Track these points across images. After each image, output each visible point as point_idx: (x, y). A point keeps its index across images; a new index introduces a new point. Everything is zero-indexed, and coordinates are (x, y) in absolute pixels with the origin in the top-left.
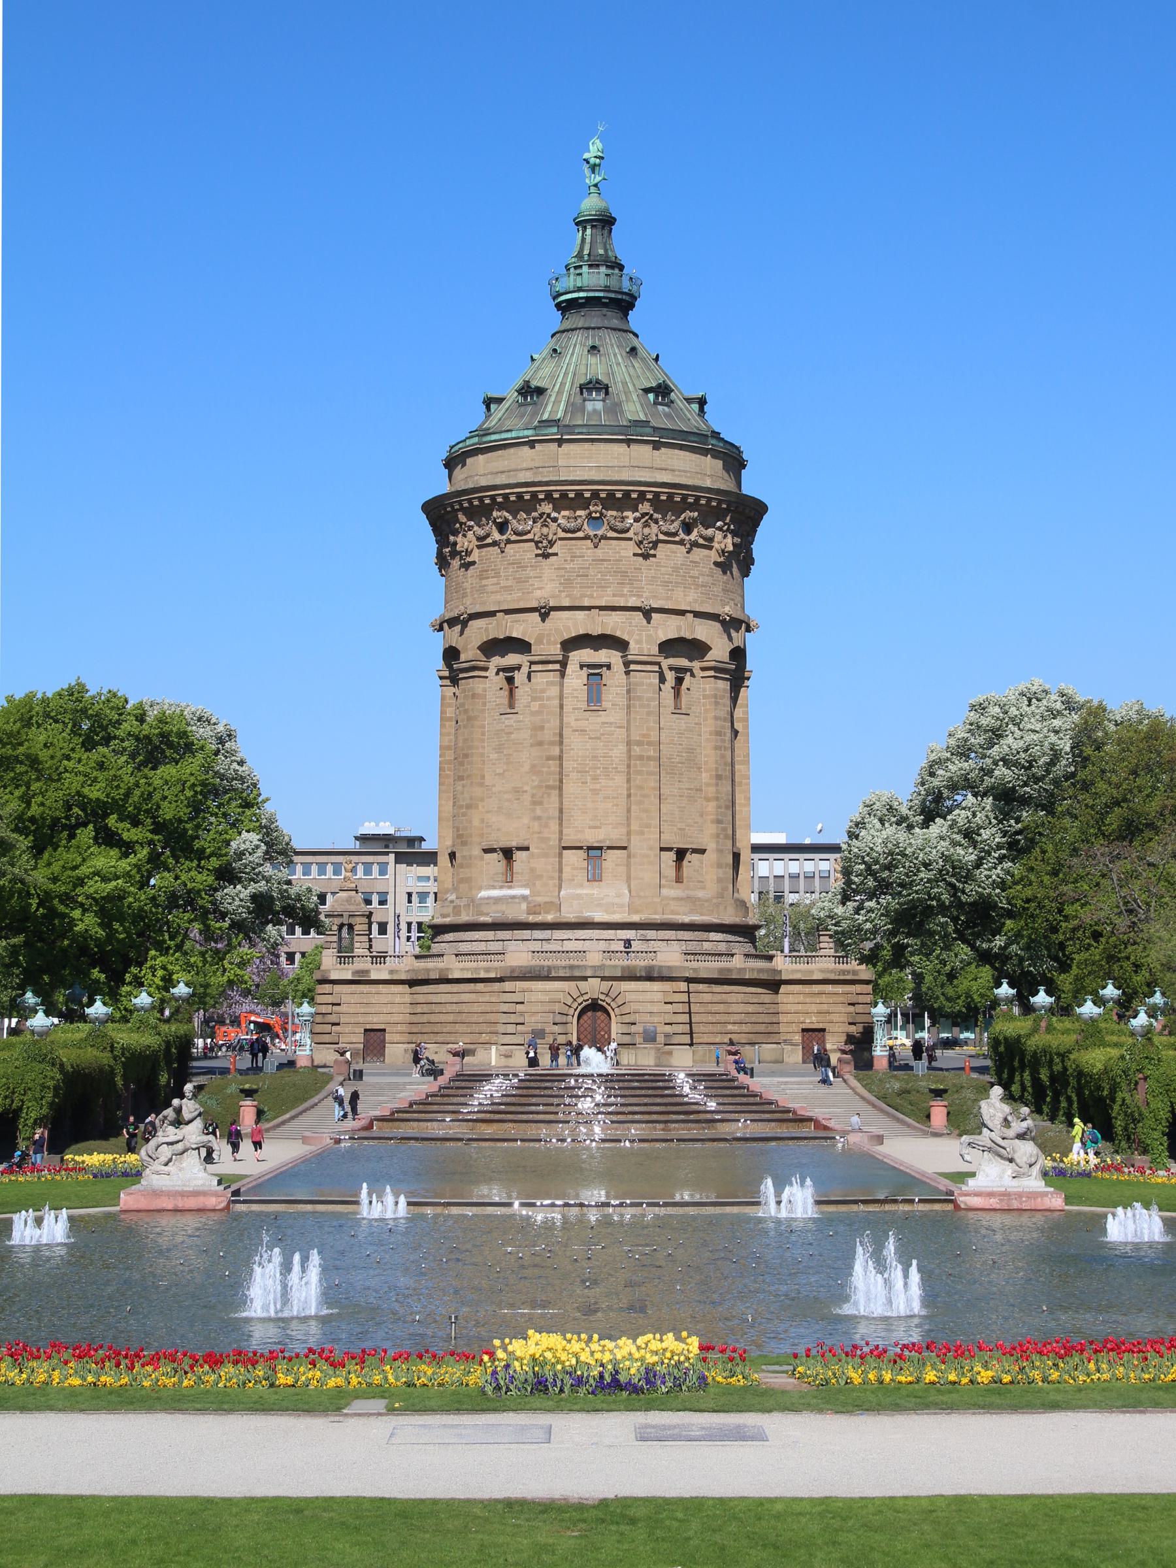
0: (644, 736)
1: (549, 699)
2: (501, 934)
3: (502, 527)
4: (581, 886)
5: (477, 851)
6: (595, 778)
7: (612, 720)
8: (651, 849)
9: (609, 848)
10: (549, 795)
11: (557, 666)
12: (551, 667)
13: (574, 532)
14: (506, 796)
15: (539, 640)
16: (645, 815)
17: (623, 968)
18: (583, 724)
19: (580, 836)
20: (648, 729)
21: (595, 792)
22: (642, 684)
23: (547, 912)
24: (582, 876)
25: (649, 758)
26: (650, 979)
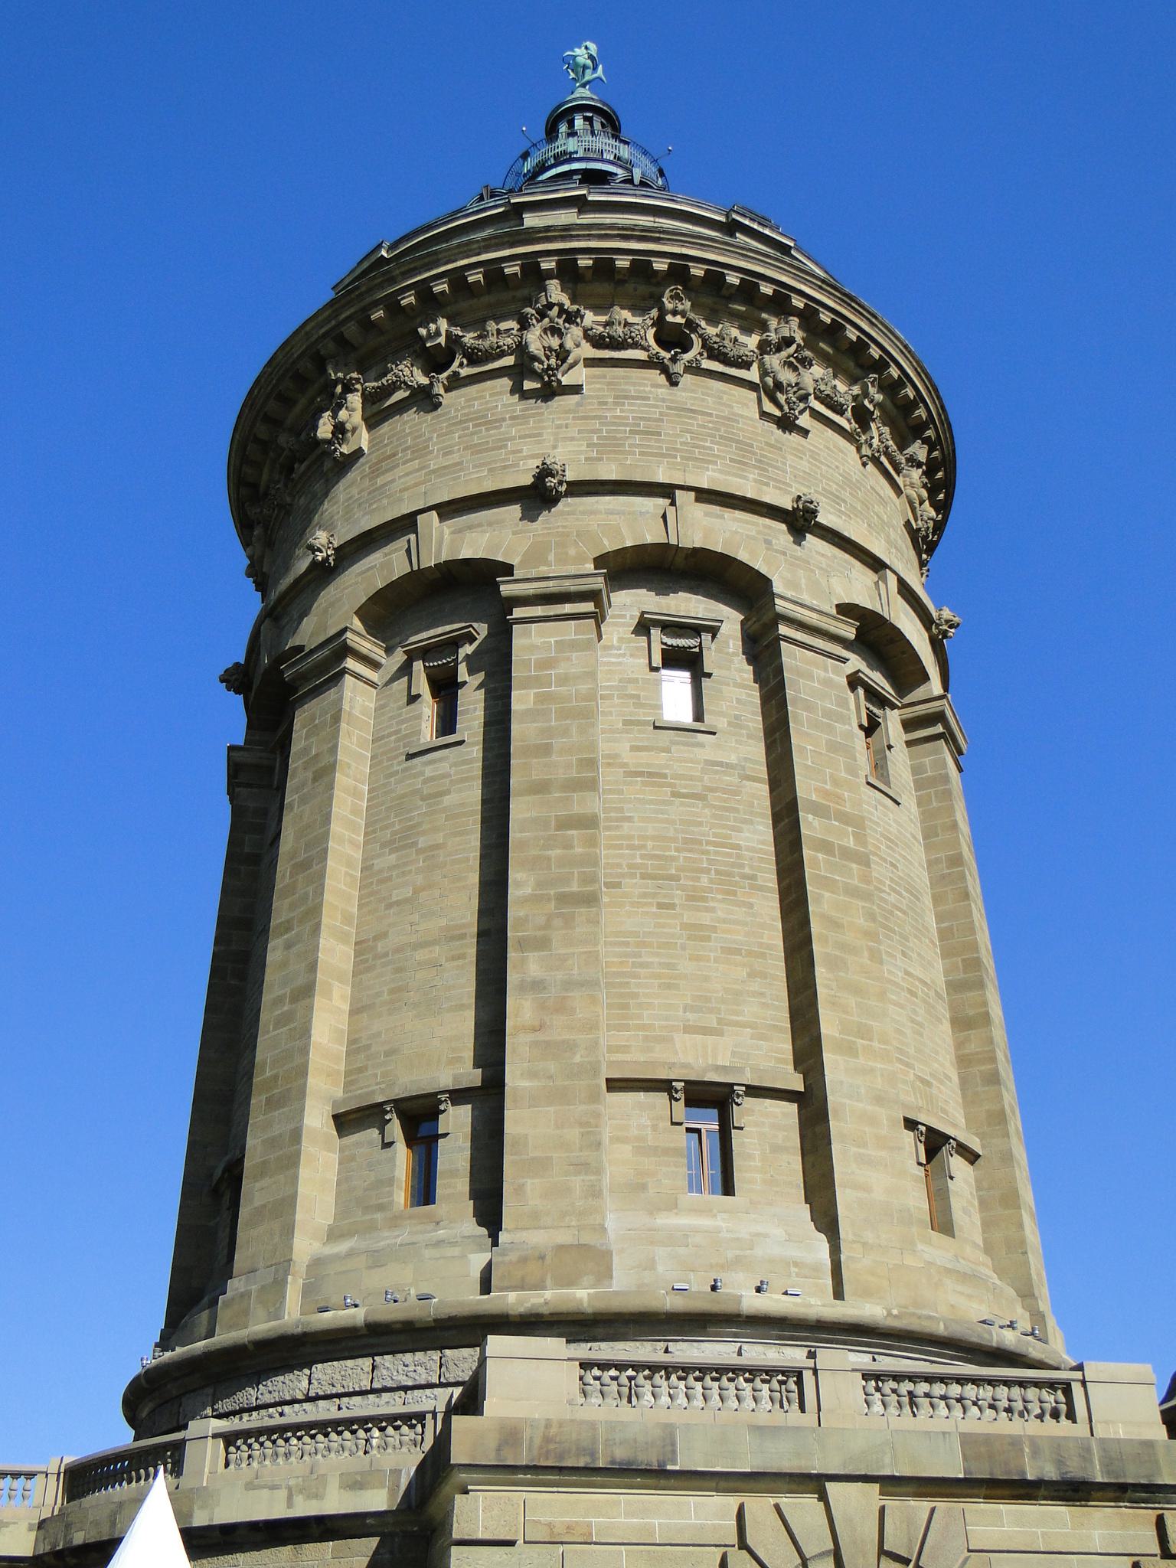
0: (827, 794)
1: (563, 680)
2: (394, 1367)
3: (436, 361)
4: (672, 1206)
5: (317, 1118)
6: (696, 897)
7: (733, 759)
8: (879, 1100)
9: (754, 1091)
10: (569, 922)
11: (588, 607)
12: (568, 608)
13: (621, 345)
14: (420, 955)
15: (536, 554)
16: (852, 1001)
17: (967, 1439)
18: (658, 760)
19: (659, 1054)
20: (836, 782)
21: (699, 933)
22: (811, 677)
23: (571, 1283)
24: (673, 1175)
25: (846, 854)
26: (1074, 1491)
